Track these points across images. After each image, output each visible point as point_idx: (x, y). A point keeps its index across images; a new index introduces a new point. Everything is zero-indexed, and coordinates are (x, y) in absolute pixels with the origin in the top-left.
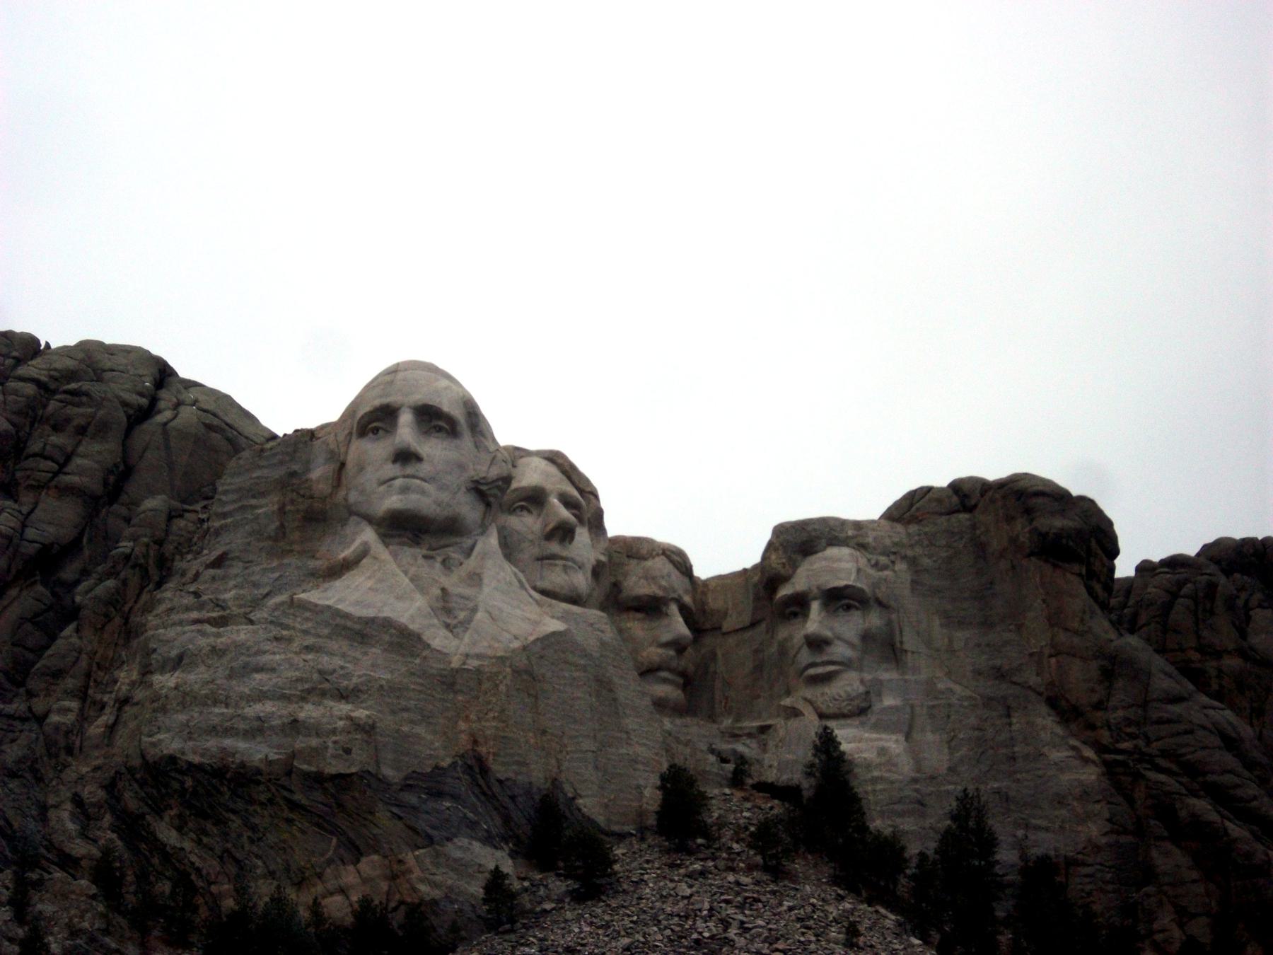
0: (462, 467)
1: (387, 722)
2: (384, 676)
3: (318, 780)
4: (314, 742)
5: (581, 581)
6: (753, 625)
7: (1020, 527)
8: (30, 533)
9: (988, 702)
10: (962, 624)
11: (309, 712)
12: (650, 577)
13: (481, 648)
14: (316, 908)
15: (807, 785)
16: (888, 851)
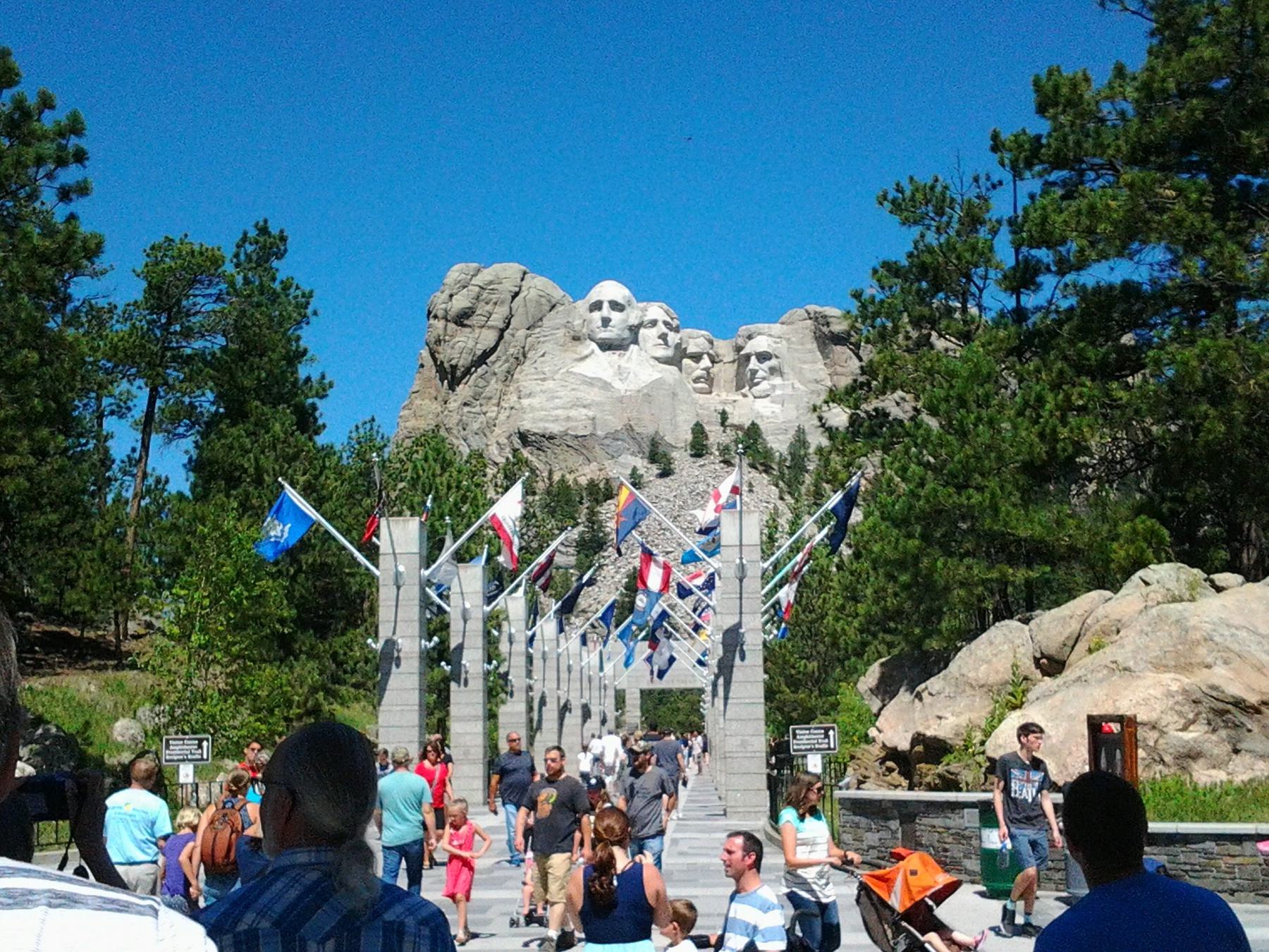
0: (625, 321)
1: (598, 416)
2: (597, 399)
3: (577, 437)
4: (574, 424)
5: (670, 352)
6: (734, 361)
7: (825, 329)
8: (479, 346)
9: (812, 392)
10: (805, 362)
11: (573, 413)
12: (697, 345)
13: (632, 387)
14: (575, 480)
15: (747, 424)
16: (768, 453)
